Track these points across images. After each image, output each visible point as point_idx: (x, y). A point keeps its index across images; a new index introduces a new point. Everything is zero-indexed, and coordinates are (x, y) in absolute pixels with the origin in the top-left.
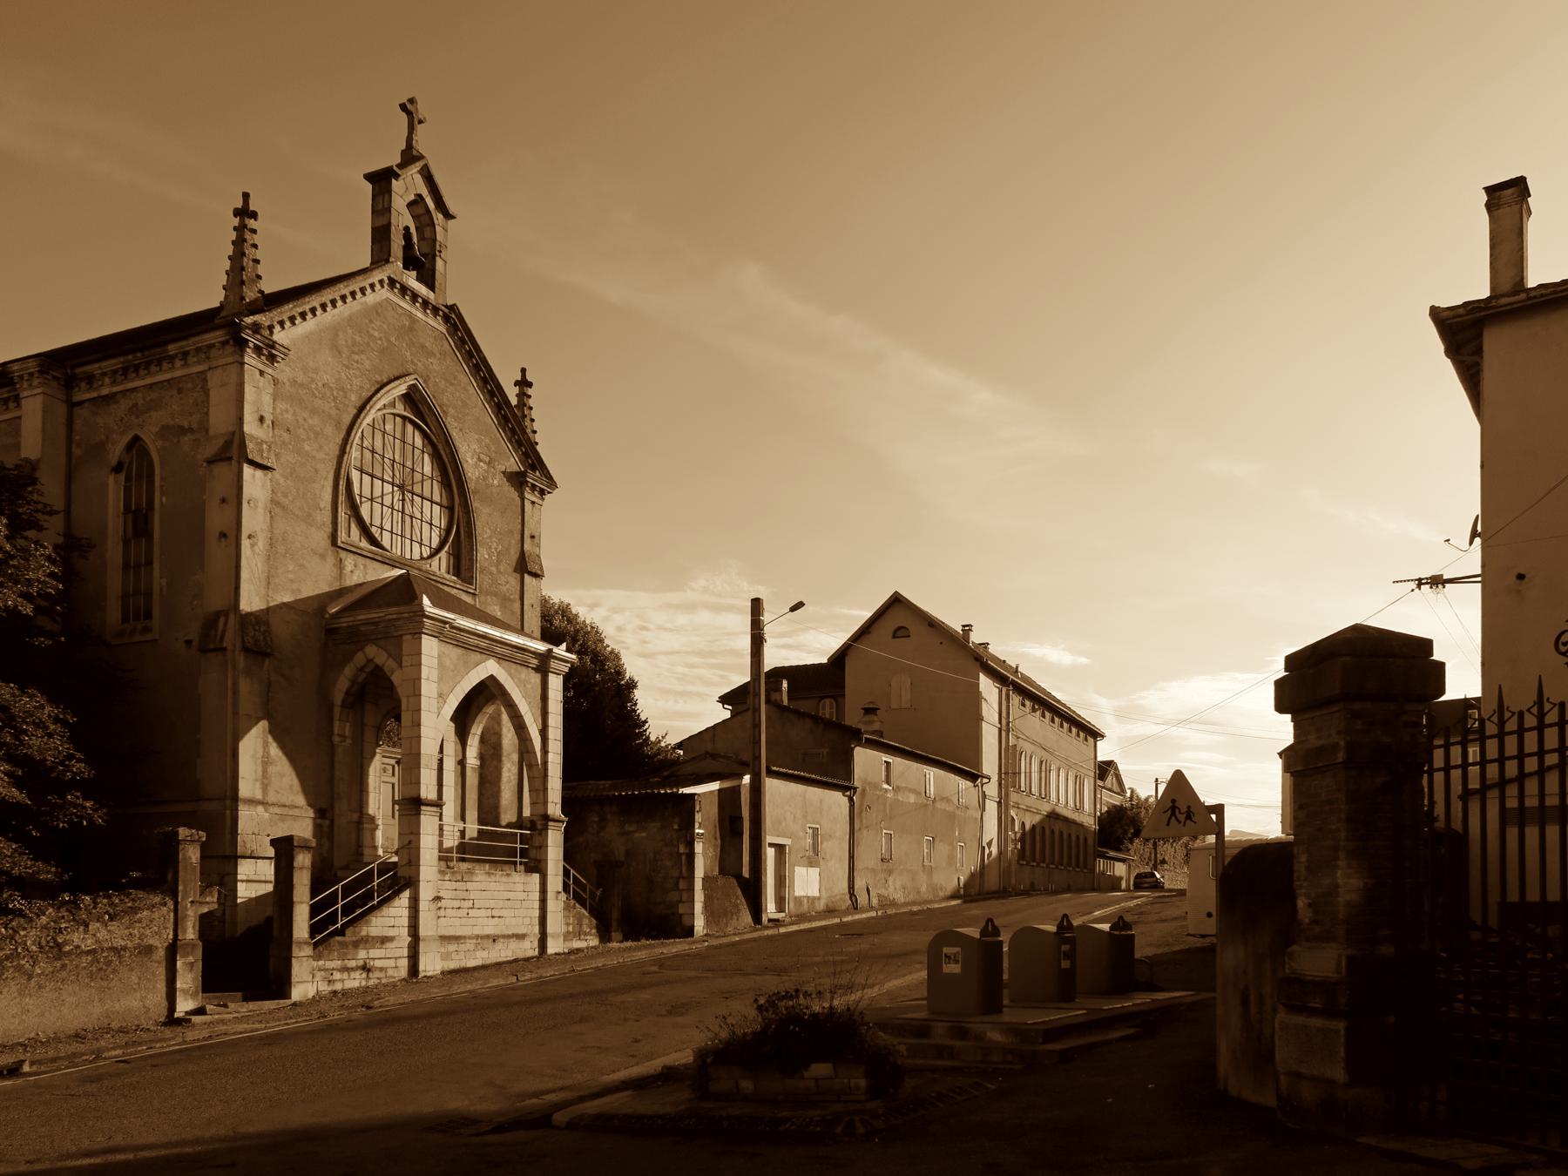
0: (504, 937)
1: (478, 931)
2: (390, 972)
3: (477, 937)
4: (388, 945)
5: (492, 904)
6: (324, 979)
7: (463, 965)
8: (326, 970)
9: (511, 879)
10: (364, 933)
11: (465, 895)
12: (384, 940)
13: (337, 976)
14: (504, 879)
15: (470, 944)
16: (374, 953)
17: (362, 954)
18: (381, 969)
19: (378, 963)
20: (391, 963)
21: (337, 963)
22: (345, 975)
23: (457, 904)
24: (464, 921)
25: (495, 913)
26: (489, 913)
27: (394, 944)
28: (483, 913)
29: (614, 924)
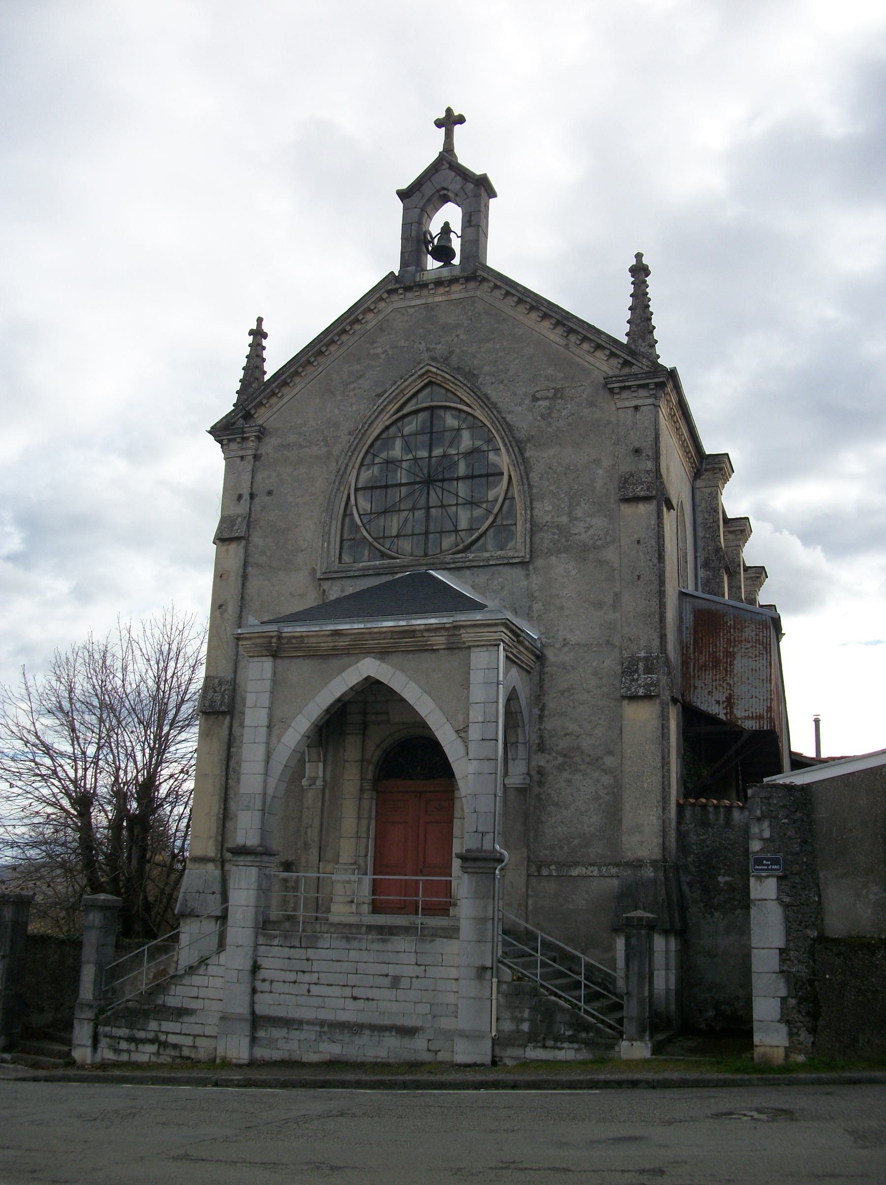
0: (373, 1028)
1: (325, 1015)
2: (186, 1052)
3: (322, 1023)
4: (186, 1019)
5: (353, 979)
6: (111, 1047)
7: (295, 1057)
8: (111, 1037)
9: (389, 946)
10: (160, 1002)
11: (305, 966)
12: (182, 1013)
13: (124, 1045)
14: (377, 946)
15: (309, 1033)
16: (167, 1026)
17: (153, 1025)
18: (175, 1046)
19: (172, 1039)
20: (189, 1041)
21: (123, 1032)
22: (133, 1047)
23: (292, 976)
24: (301, 1000)
25: (357, 992)
26: (348, 992)
27: (192, 1019)
28: (337, 991)
29: (630, 1028)
